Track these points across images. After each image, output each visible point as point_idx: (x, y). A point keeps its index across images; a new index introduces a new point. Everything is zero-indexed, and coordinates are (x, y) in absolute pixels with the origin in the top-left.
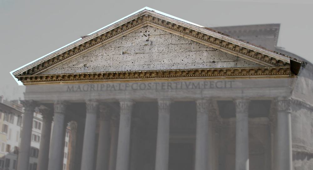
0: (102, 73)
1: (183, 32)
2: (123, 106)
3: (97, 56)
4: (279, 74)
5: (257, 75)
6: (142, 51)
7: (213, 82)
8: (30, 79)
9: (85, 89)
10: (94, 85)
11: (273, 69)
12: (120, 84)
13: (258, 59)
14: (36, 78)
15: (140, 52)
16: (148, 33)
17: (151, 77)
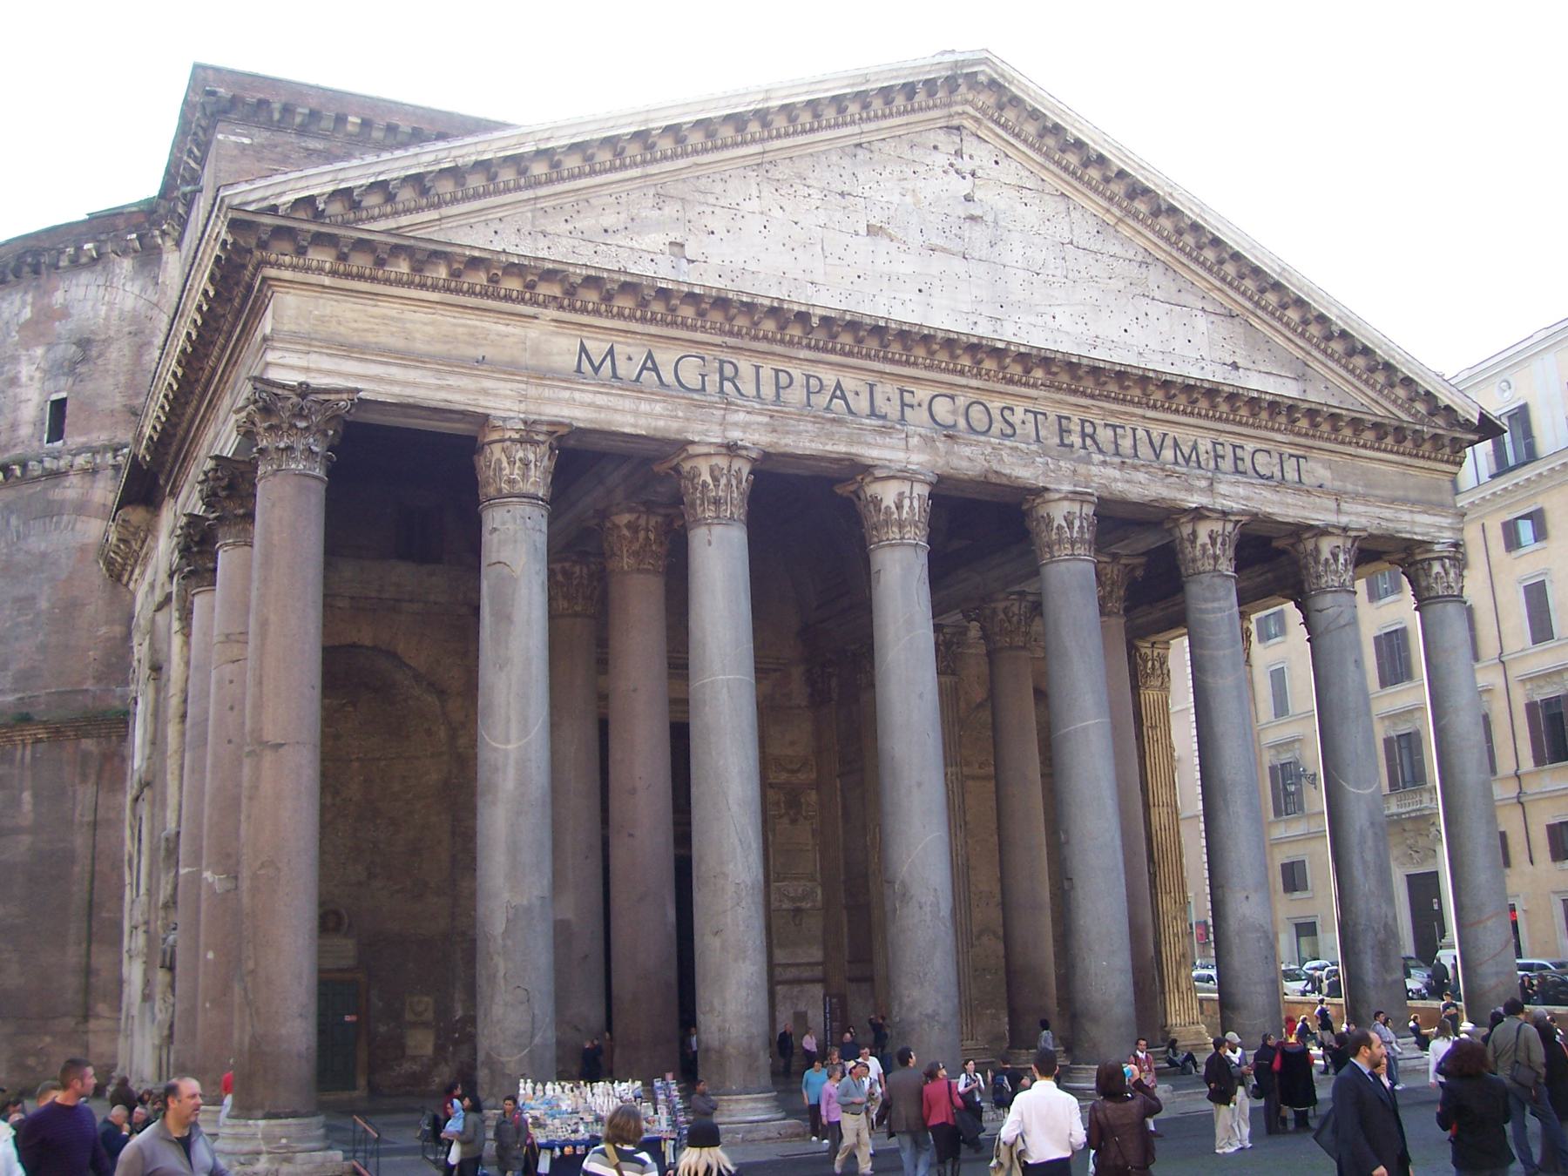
0: (819, 312)
1: (1119, 206)
2: (907, 503)
4: (1435, 459)
5: (1378, 449)
6: (954, 245)
9: (690, 377)
12: (871, 386)
13: (1373, 387)
16: (965, 165)
17: (1026, 385)
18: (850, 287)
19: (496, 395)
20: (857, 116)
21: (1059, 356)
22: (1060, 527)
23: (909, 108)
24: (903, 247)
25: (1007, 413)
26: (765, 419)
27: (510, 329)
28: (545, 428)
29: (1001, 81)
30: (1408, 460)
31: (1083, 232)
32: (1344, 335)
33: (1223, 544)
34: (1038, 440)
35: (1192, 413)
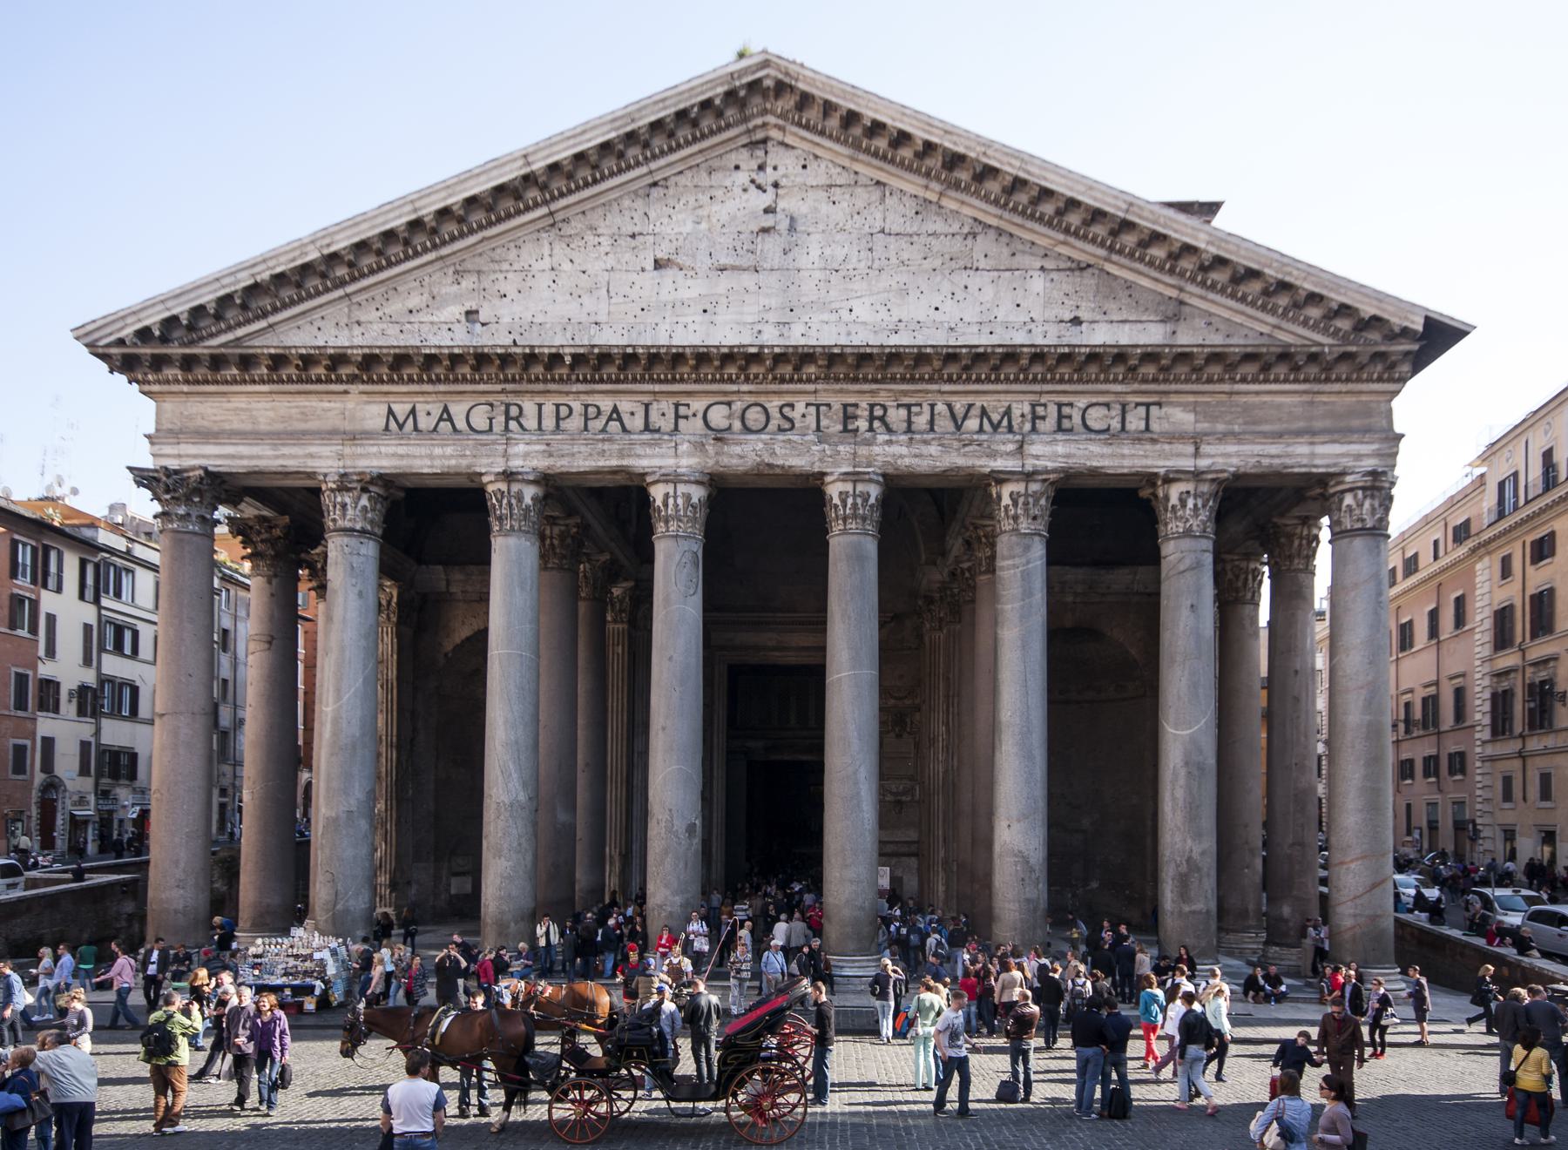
0: (567, 350)
2: (671, 501)
3: (525, 272)
4: (1359, 380)
5: (1266, 381)
6: (746, 261)
7: (1071, 405)
8: (182, 368)
9: (479, 421)
10: (520, 408)
11: (1346, 357)
12: (647, 406)
14: (217, 362)
15: (737, 263)
16: (768, 177)
17: (800, 381)
18: (633, 320)
19: (320, 457)
20: (640, 158)
21: (819, 350)
22: (836, 506)
23: (698, 135)
24: (693, 273)
26: (543, 447)
27: (332, 405)
28: (355, 478)
29: (787, 80)
30: (1316, 387)
31: (897, 215)
32: (1220, 262)
34: (818, 428)
35: (998, 381)
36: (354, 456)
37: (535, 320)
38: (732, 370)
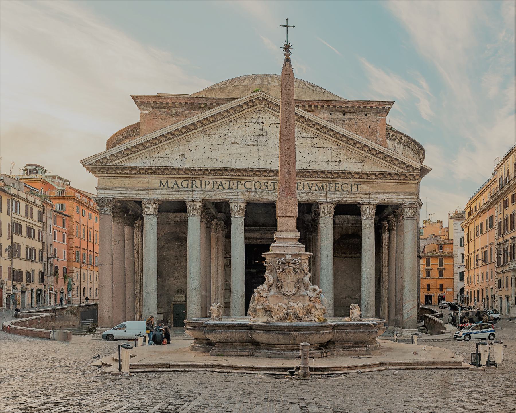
0: (209, 168)
4: (408, 180)
5: (386, 179)
6: (255, 143)
9: (185, 185)
10: (196, 181)
12: (229, 182)
13: (387, 161)
17: (269, 176)
18: (225, 158)
19: (142, 194)
25: (266, 184)
33: (327, 210)
34: (274, 189)
35: (320, 177)
36: (151, 194)
37: (200, 158)
38: (251, 173)
